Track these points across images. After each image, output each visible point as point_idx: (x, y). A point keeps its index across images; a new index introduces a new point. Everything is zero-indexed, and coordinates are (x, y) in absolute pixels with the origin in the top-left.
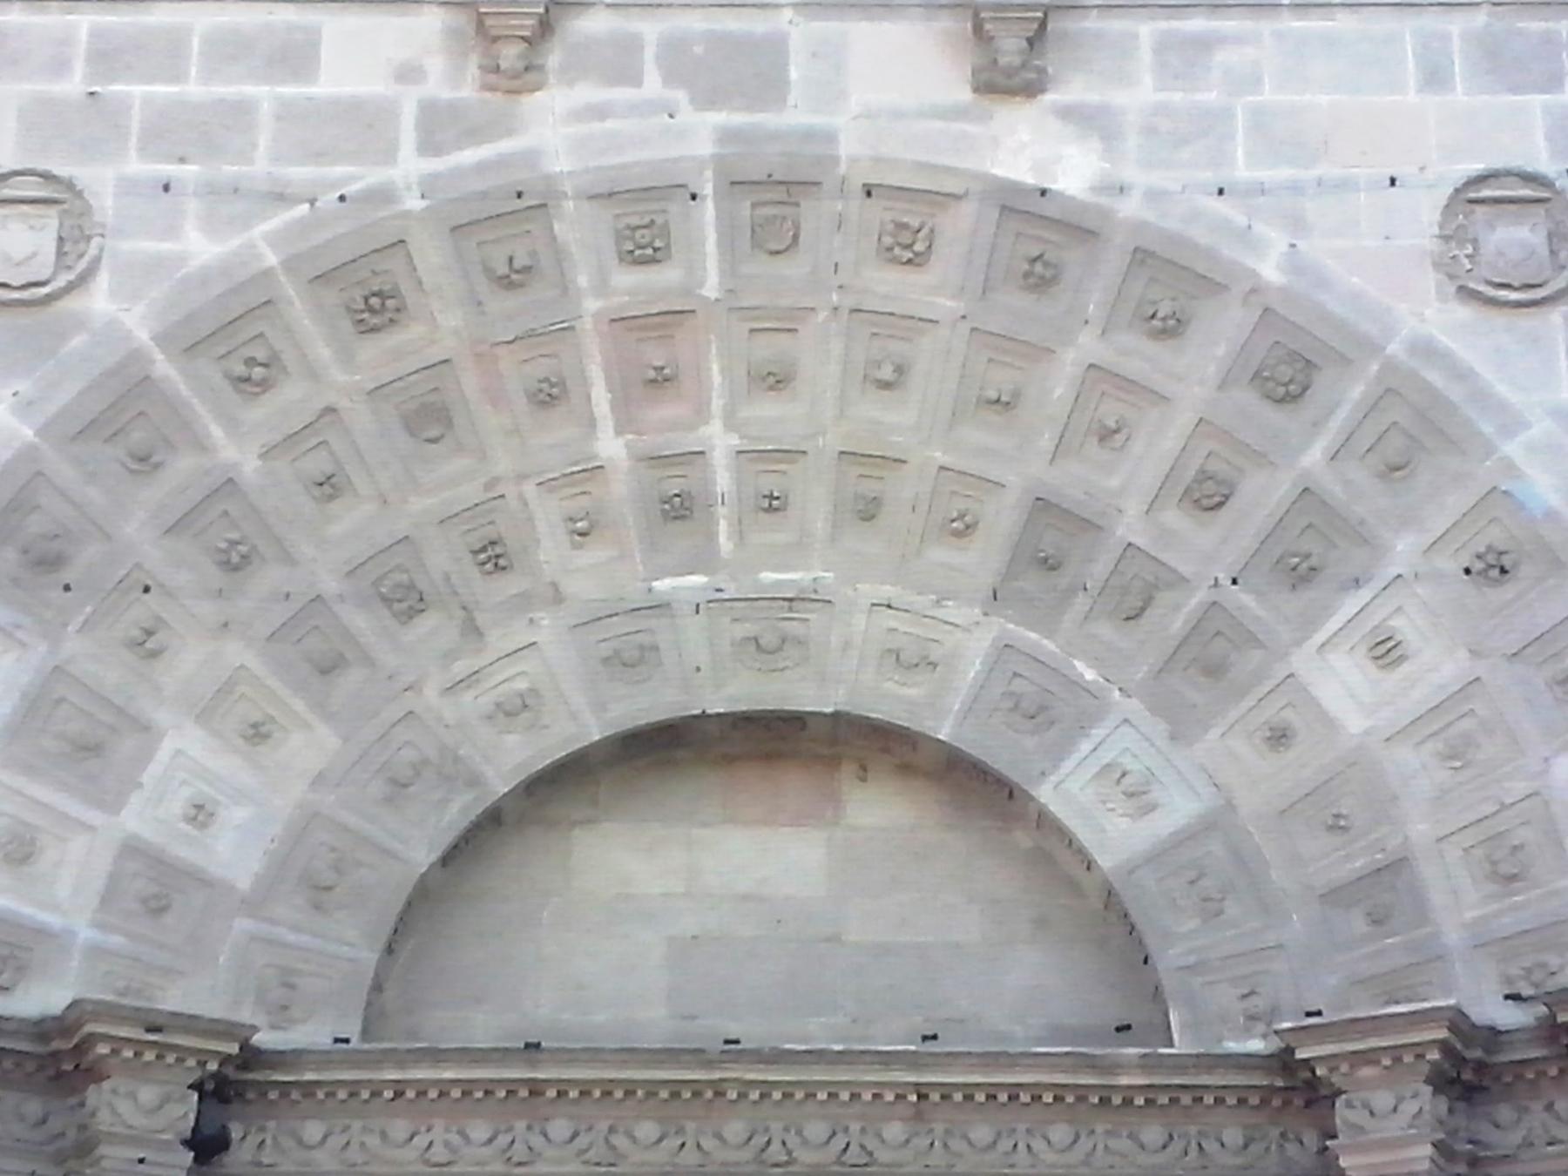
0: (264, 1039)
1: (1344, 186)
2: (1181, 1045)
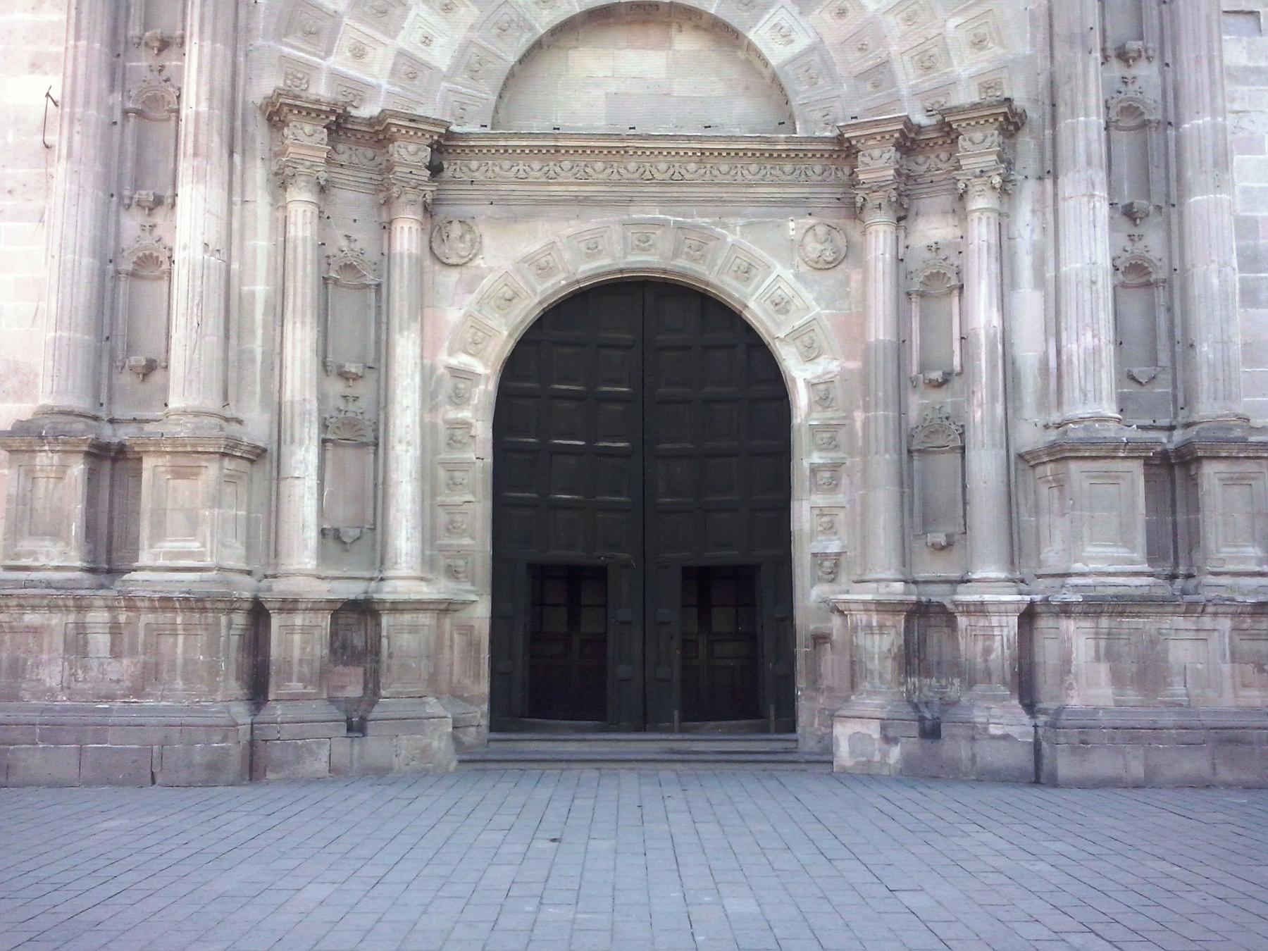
0: (454, 128)
2: (800, 133)
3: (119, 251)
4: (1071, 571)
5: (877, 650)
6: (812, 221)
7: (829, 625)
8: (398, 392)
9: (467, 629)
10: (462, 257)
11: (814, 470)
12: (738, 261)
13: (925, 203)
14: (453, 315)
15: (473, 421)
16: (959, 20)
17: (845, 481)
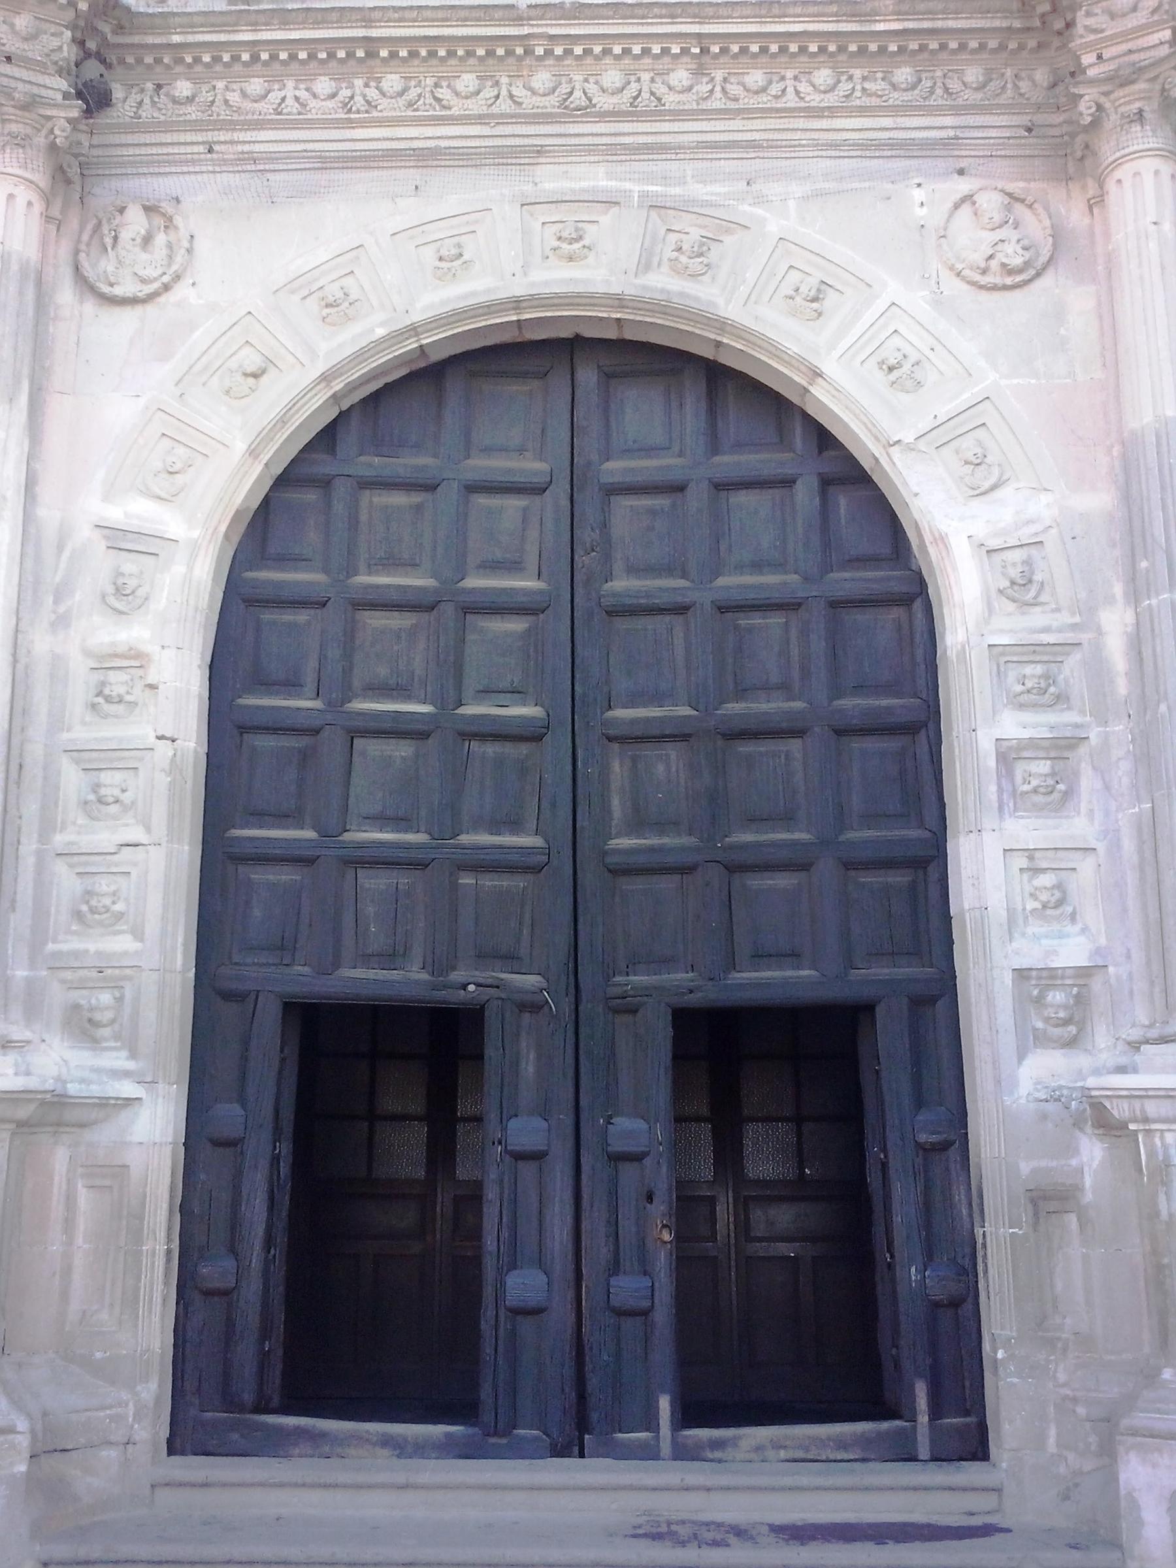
6: (964, 186)
7: (1074, 1162)
10: (144, 281)
12: (794, 276)
15: (152, 649)
17: (1088, 782)
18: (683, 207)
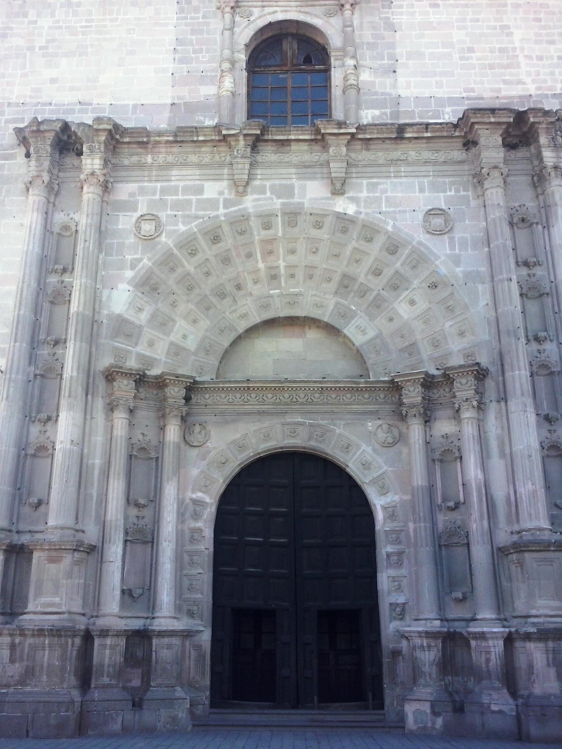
0: (198, 379)
1: (404, 212)
3: (27, 444)
4: (530, 614)
5: (427, 660)
6: (380, 422)
7: (401, 645)
8: (165, 513)
9: (198, 648)
10: (200, 442)
11: (388, 555)
13: (439, 413)
14: (195, 472)
15: (203, 528)
16: (451, 323)
17: (405, 561)
18: (319, 425)
